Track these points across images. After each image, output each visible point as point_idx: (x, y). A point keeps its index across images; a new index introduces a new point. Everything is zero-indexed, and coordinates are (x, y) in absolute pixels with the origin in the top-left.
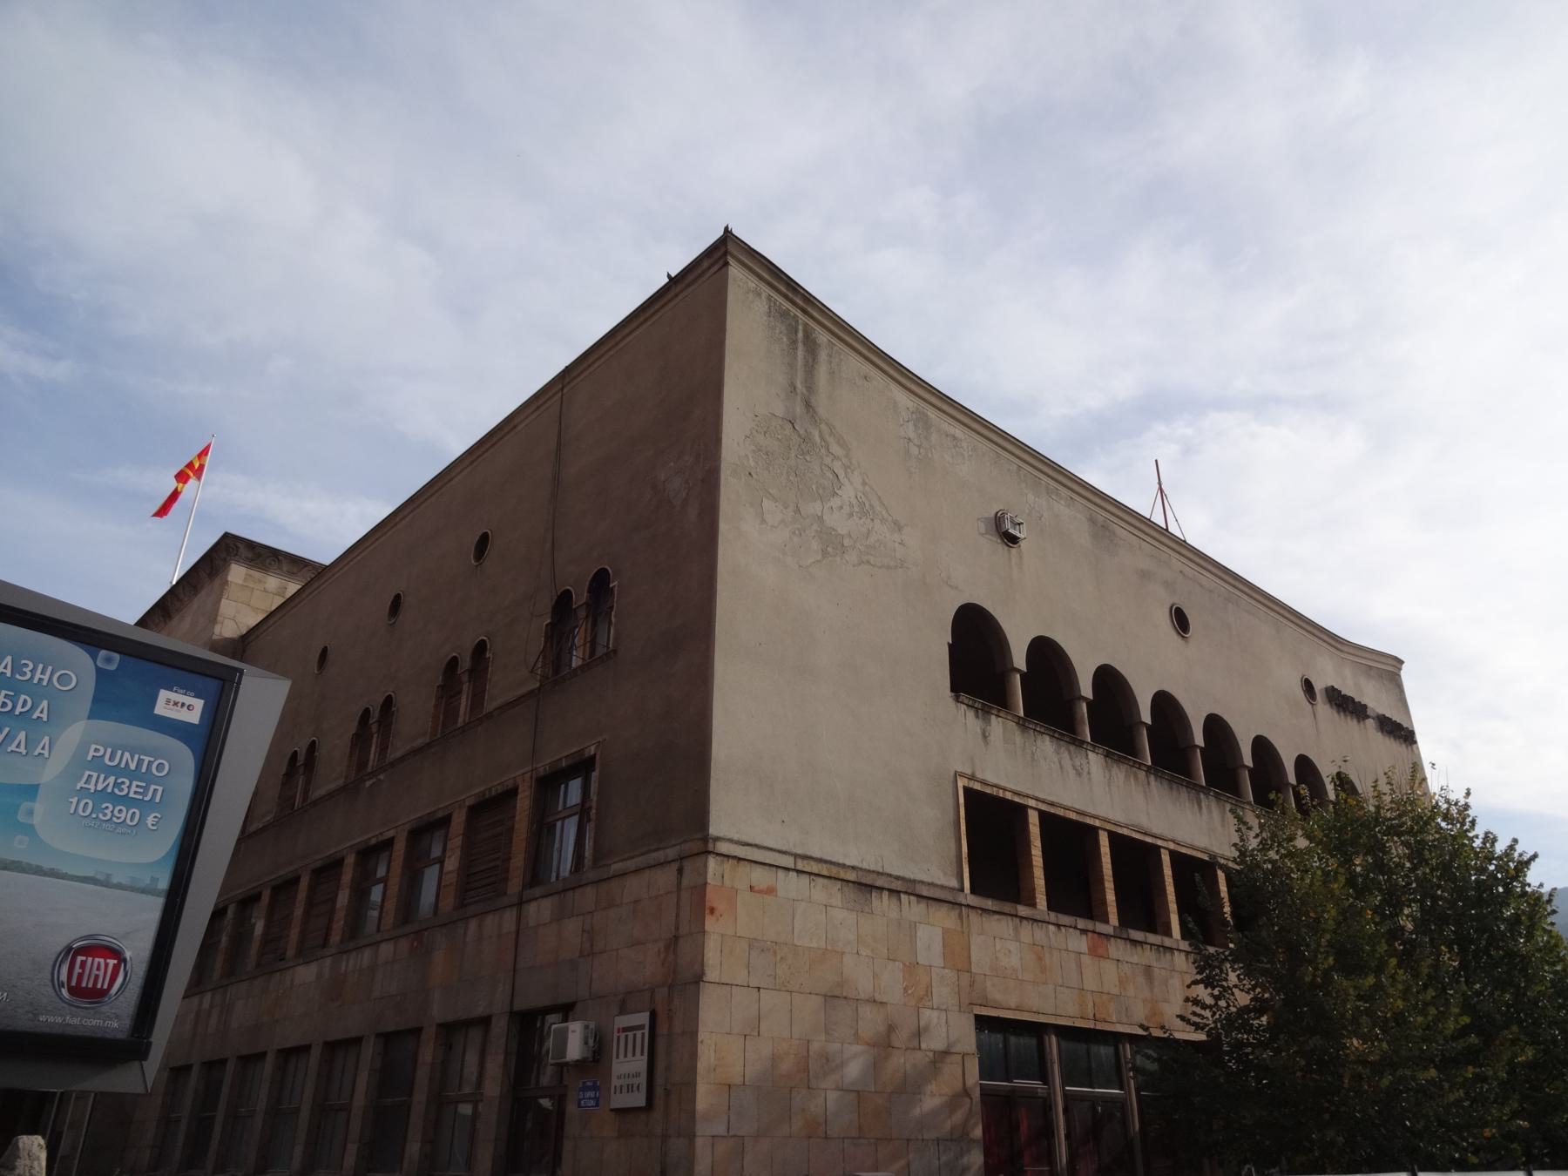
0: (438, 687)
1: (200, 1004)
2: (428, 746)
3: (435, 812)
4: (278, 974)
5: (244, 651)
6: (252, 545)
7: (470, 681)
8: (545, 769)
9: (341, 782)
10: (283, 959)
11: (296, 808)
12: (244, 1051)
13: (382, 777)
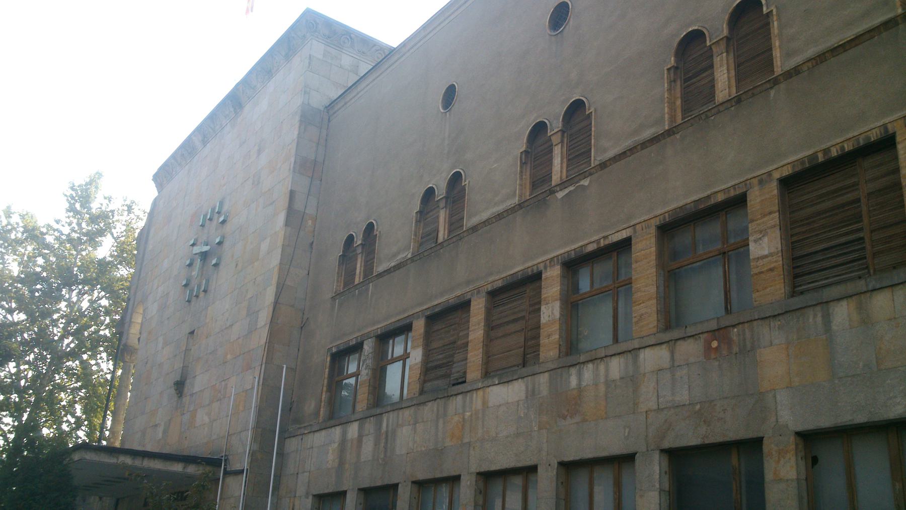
0: (669, 70)
1: (344, 434)
2: (670, 133)
3: (709, 197)
4: (460, 397)
5: (329, 121)
6: (329, 23)
7: (727, 52)
8: (665, 217)
9: (516, 200)
10: (464, 382)
11: (440, 239)
12: (421, 476)
13: (585, 182)
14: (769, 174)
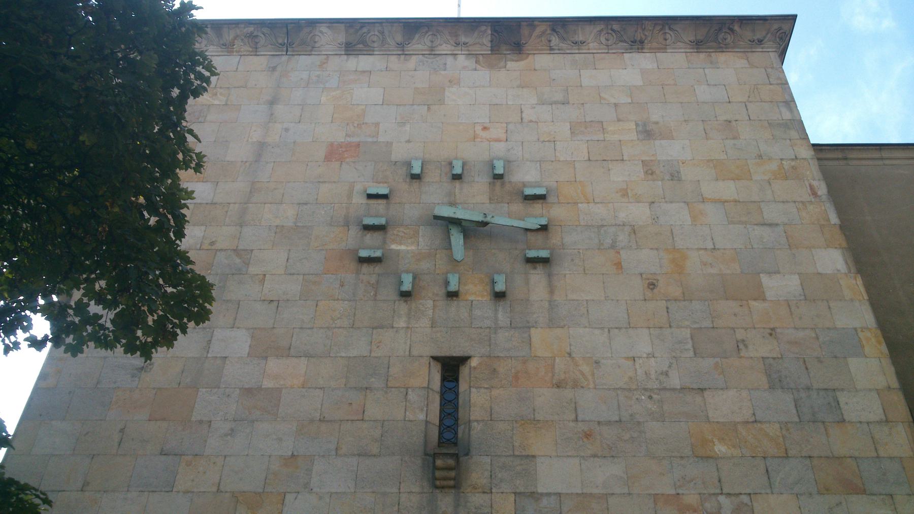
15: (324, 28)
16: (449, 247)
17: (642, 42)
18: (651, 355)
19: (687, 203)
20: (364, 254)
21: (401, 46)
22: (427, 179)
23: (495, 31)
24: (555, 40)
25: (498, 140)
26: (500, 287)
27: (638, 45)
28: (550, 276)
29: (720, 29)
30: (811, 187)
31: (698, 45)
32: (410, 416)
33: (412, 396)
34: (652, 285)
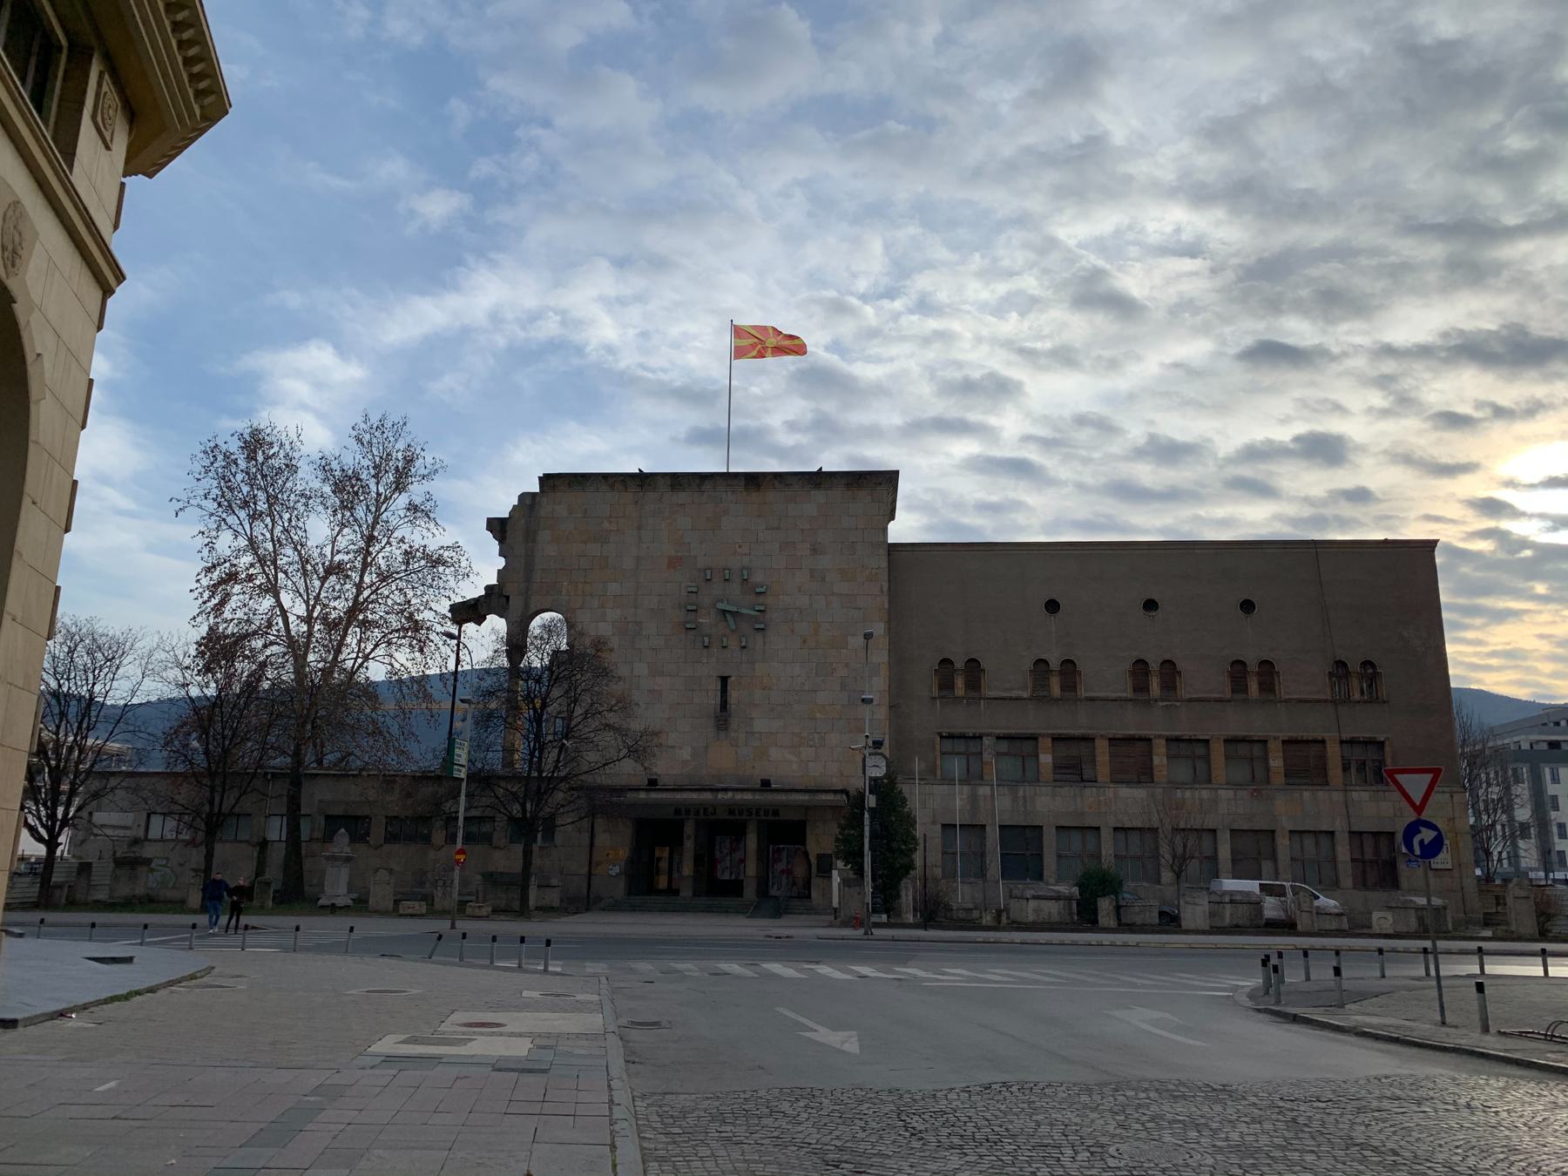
14: (1278, 737)
15: (659, 478)
16: (727, 620)
17: (820, 484)
18: (799, 676)
19: (825, 595)
20: (688, 626)
21: (699, 486)
22: (713, 580)
23: (746, 479)
24: (776, 482)
25: (746, 555)
26: (743, 644)
27: (818, 486)
28: (764, 636)
29: (860, 478)
30: (882, 587)
31: (848, 486)
32: (710, 702)
33: (710, 693)
34: (804, 642)
